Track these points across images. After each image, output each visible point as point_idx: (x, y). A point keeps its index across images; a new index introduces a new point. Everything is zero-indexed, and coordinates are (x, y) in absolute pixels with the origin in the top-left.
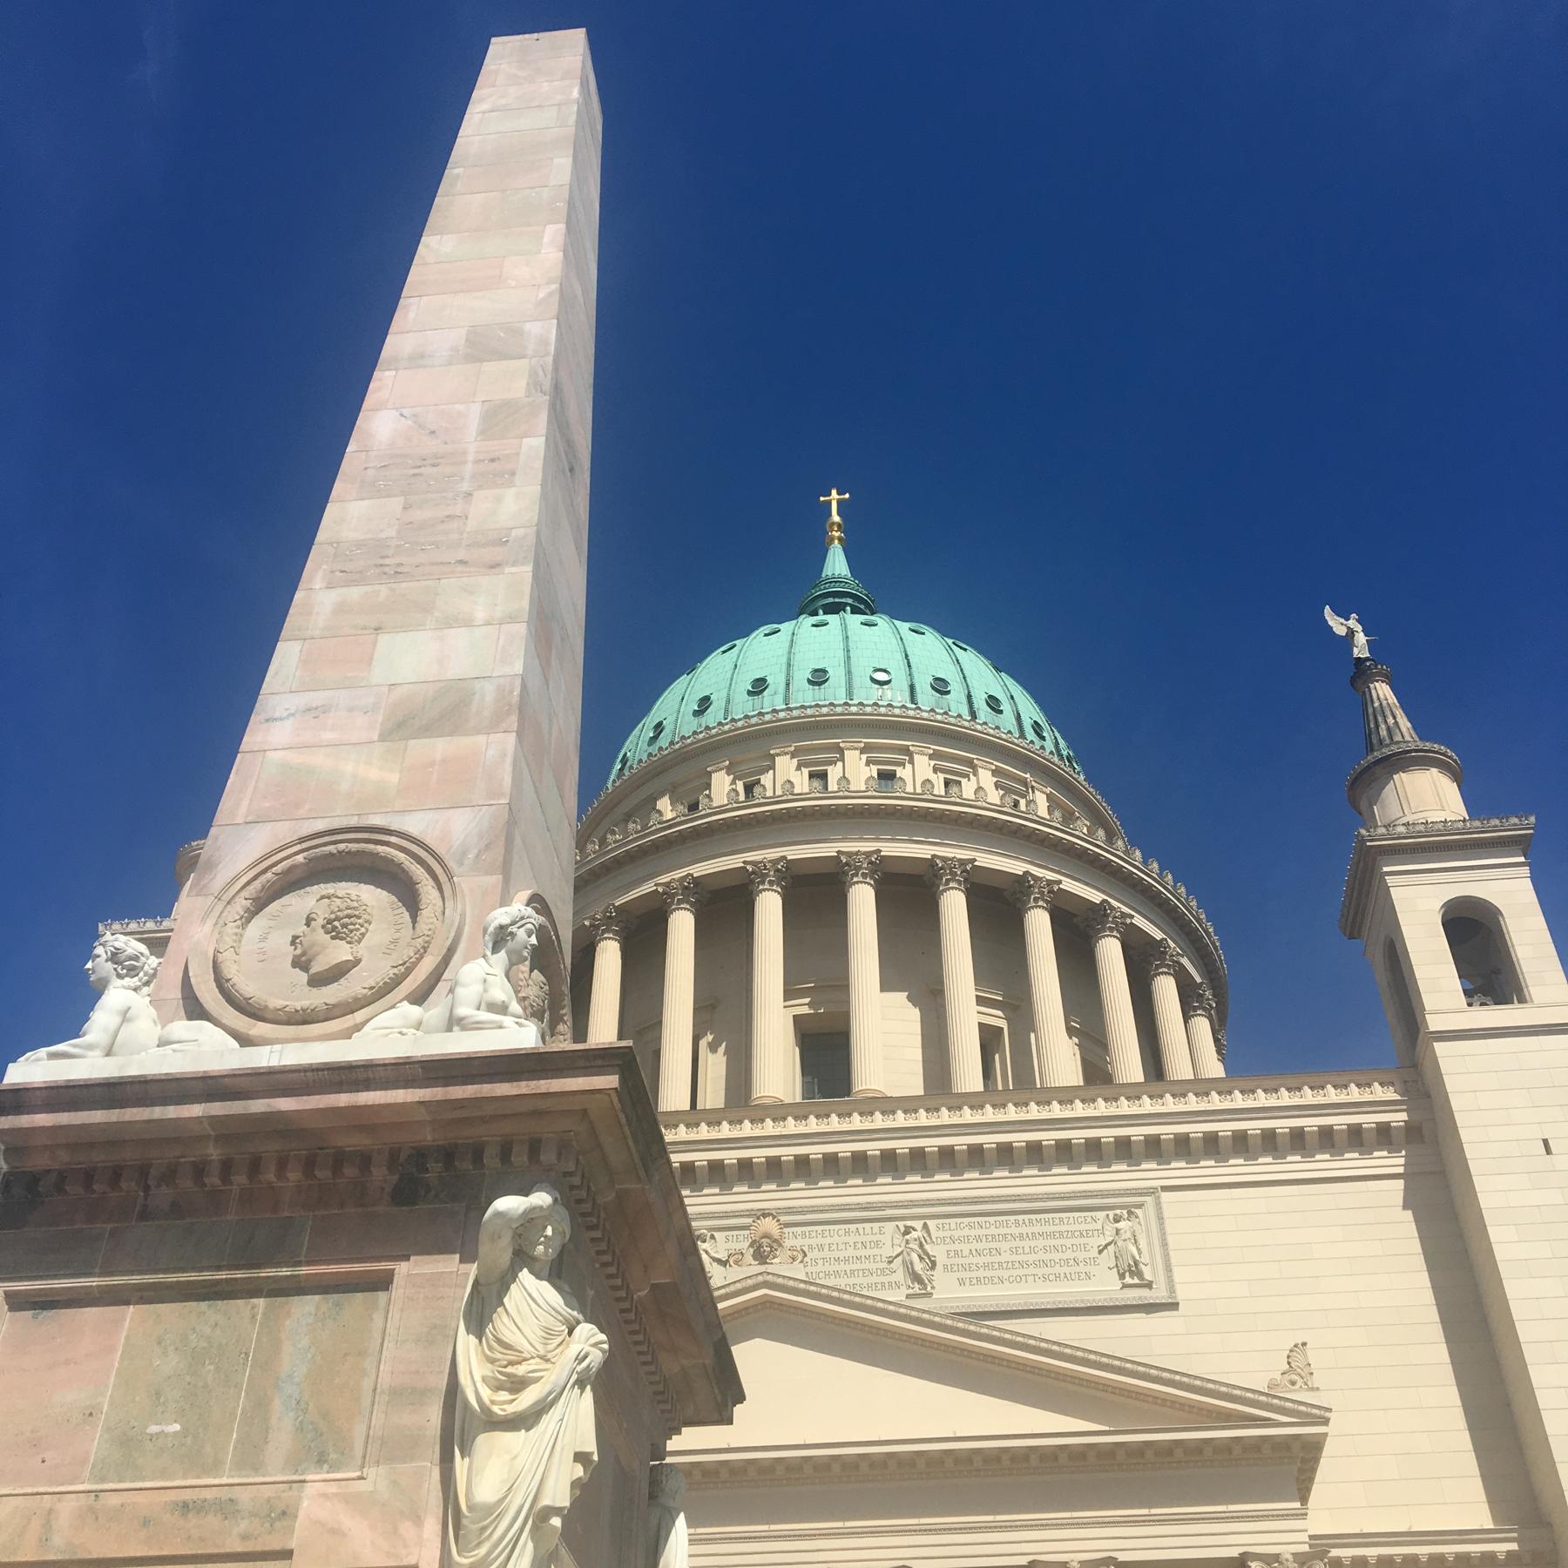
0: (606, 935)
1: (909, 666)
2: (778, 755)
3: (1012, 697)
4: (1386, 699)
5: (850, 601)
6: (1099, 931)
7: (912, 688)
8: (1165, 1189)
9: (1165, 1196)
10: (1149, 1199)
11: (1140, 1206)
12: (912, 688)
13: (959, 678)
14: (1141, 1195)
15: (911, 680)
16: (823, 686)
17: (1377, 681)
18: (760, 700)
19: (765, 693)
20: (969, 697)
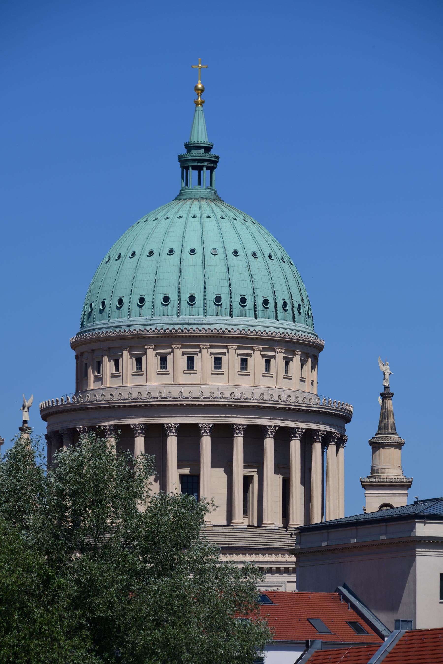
0: (110, 436)
1: (231, 292)
2: (175, 348)
3: (275, 293)
4: (388, 409)
5: (205, 164)
6: (292, 437)
7: (231, 306)
8: (288, 582)
9: (288, 584)
10: (283, 585)
11: (281, 587)
12: (231, 306)
13: (251, 293)
14: (281, 583)
15: (231, 302)
16: (193, 306)
17: (387, 399)
18: (167, 309)
19: (169, 305)
20: (255, 305)
